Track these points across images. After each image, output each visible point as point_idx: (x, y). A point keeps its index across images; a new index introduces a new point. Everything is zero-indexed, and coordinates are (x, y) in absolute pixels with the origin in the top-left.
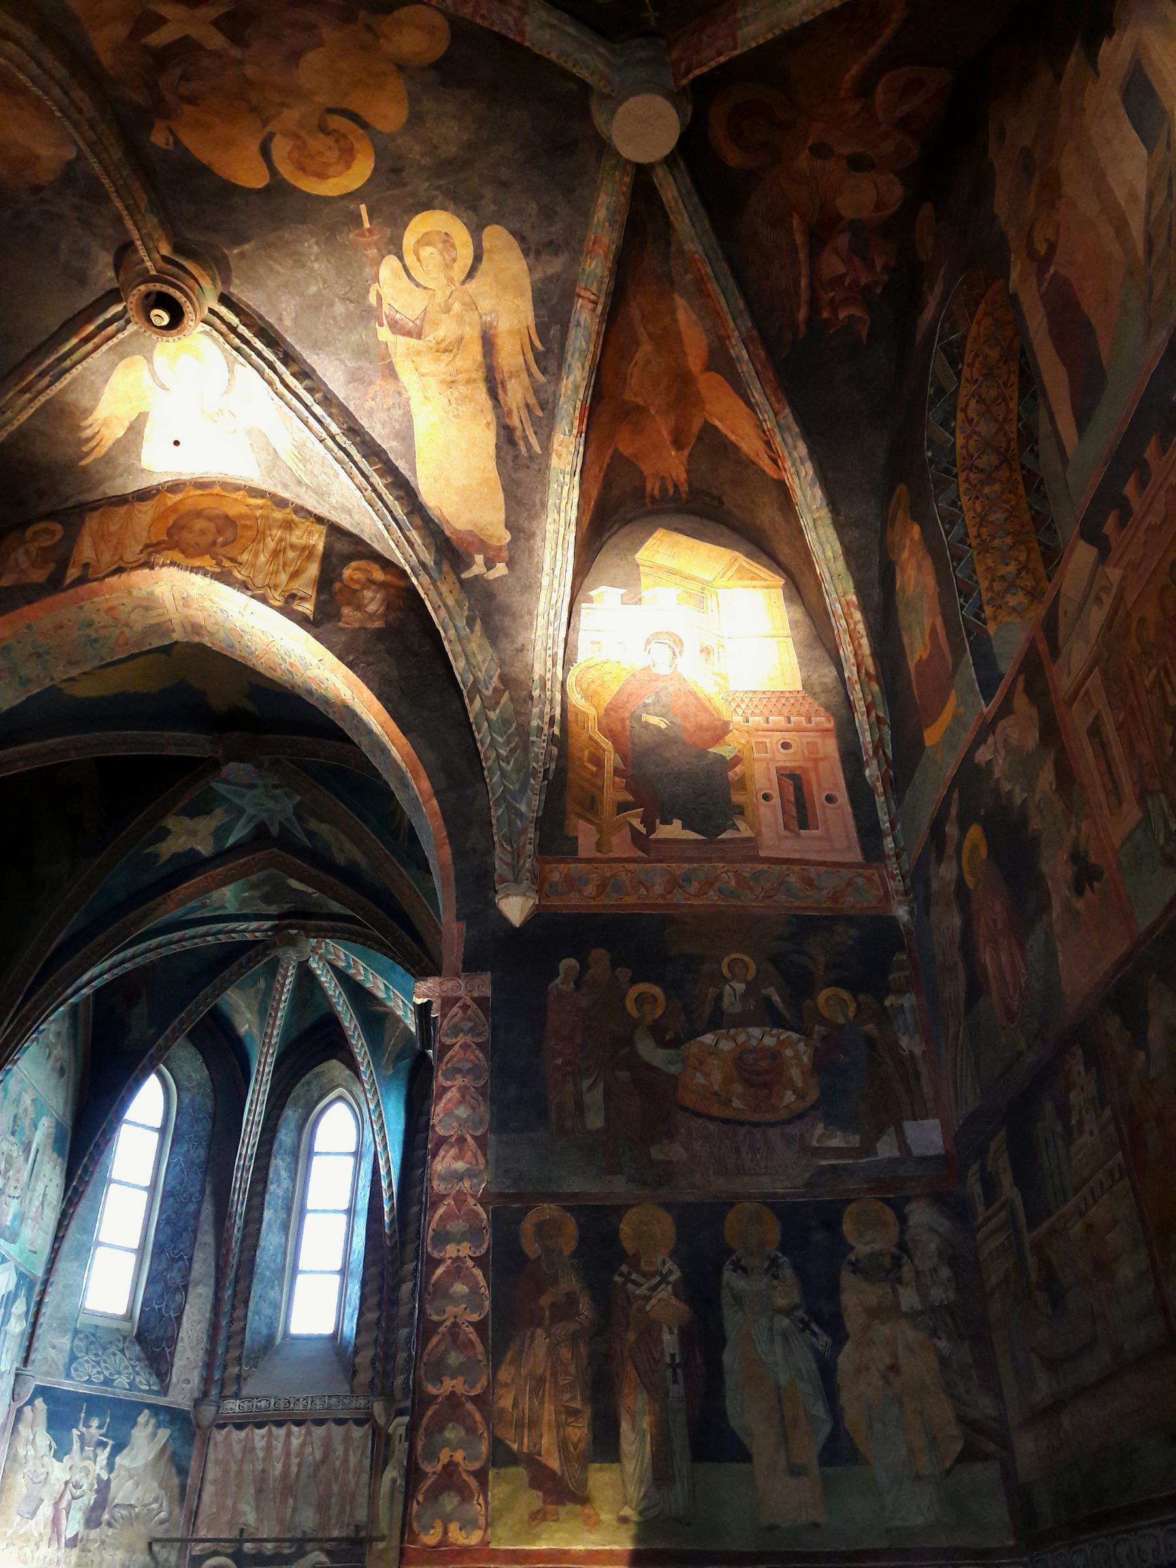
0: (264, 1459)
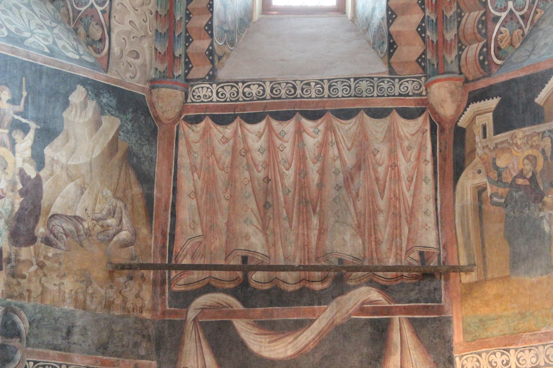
0: (267, 165)
